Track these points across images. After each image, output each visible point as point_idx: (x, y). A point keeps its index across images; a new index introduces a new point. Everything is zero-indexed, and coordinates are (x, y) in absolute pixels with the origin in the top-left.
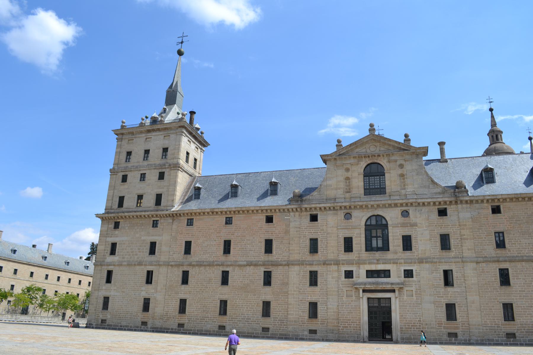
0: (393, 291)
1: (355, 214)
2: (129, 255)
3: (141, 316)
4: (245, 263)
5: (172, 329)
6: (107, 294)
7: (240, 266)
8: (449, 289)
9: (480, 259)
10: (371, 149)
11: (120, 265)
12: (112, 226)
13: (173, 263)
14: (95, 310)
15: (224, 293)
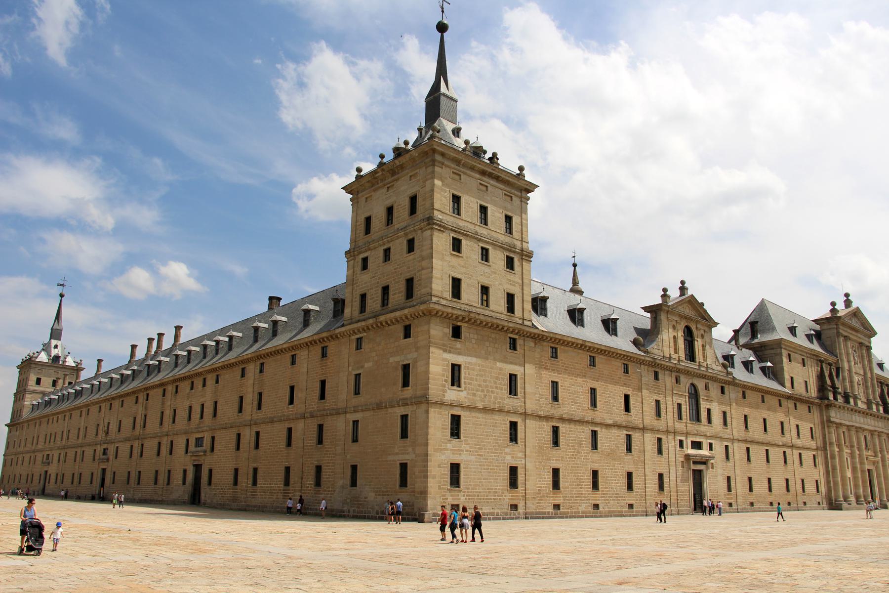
0: (704, 463)
1: (683, 379)
2: (483, 391)
3: (508, 497)
4: (610, 422)
5: (548, 513)
6: (456, 459)
7: (608, 426)
8: (728, 464)
9: (740, 438)
10: (688, 311)
11: (472, 408)
12: (449, 331)
13: (541, 413)
14: (440, 488)
15: (595, 461)
